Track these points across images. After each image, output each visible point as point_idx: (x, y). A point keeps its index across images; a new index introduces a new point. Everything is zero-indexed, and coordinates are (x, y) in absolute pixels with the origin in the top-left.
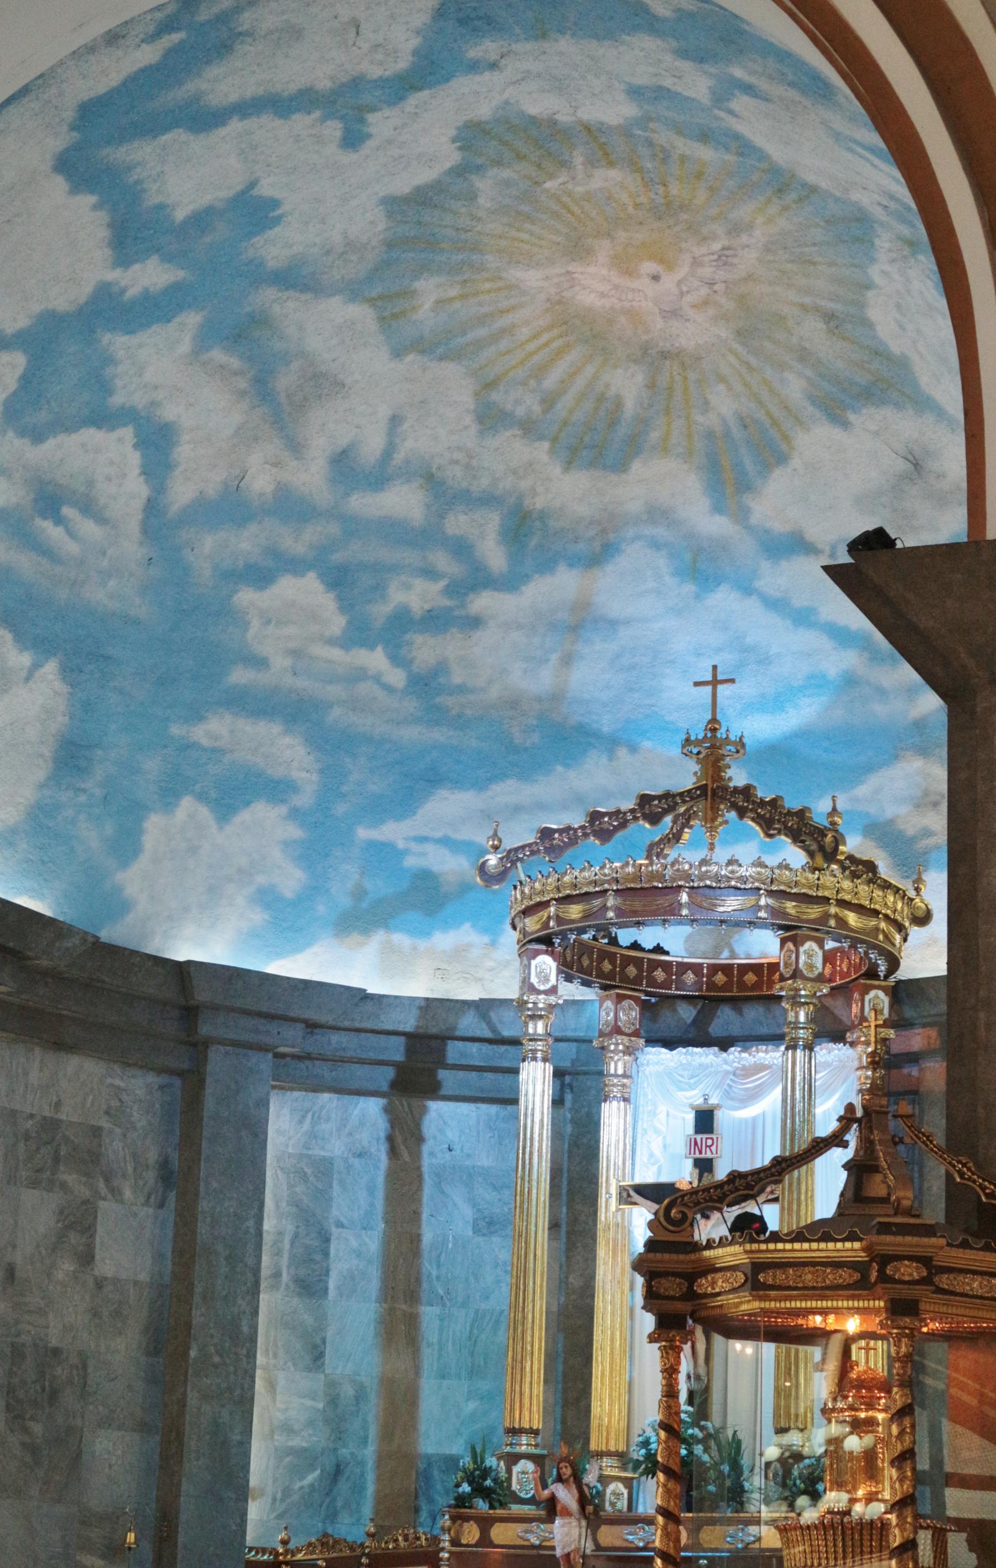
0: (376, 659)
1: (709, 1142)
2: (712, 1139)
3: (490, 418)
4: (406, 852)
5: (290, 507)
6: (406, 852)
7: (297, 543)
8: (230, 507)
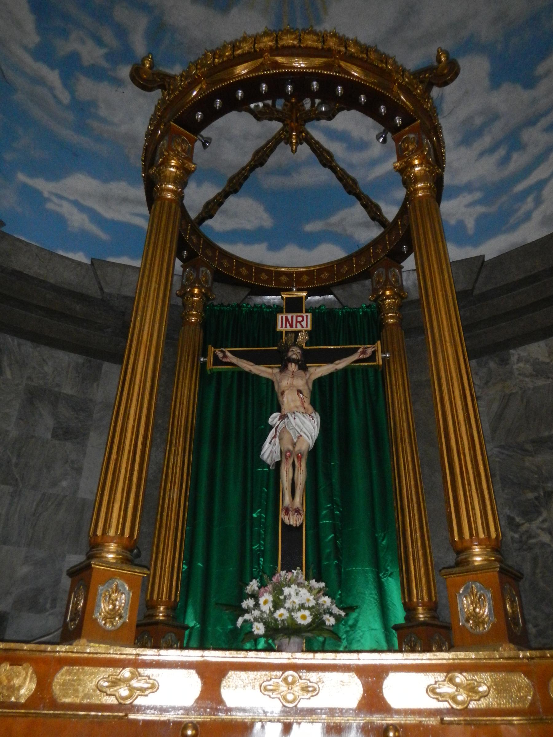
0: (54, 77)
1: (300, 319)
2: (303, 317)
4: (48, 200)
6: (48, 200)
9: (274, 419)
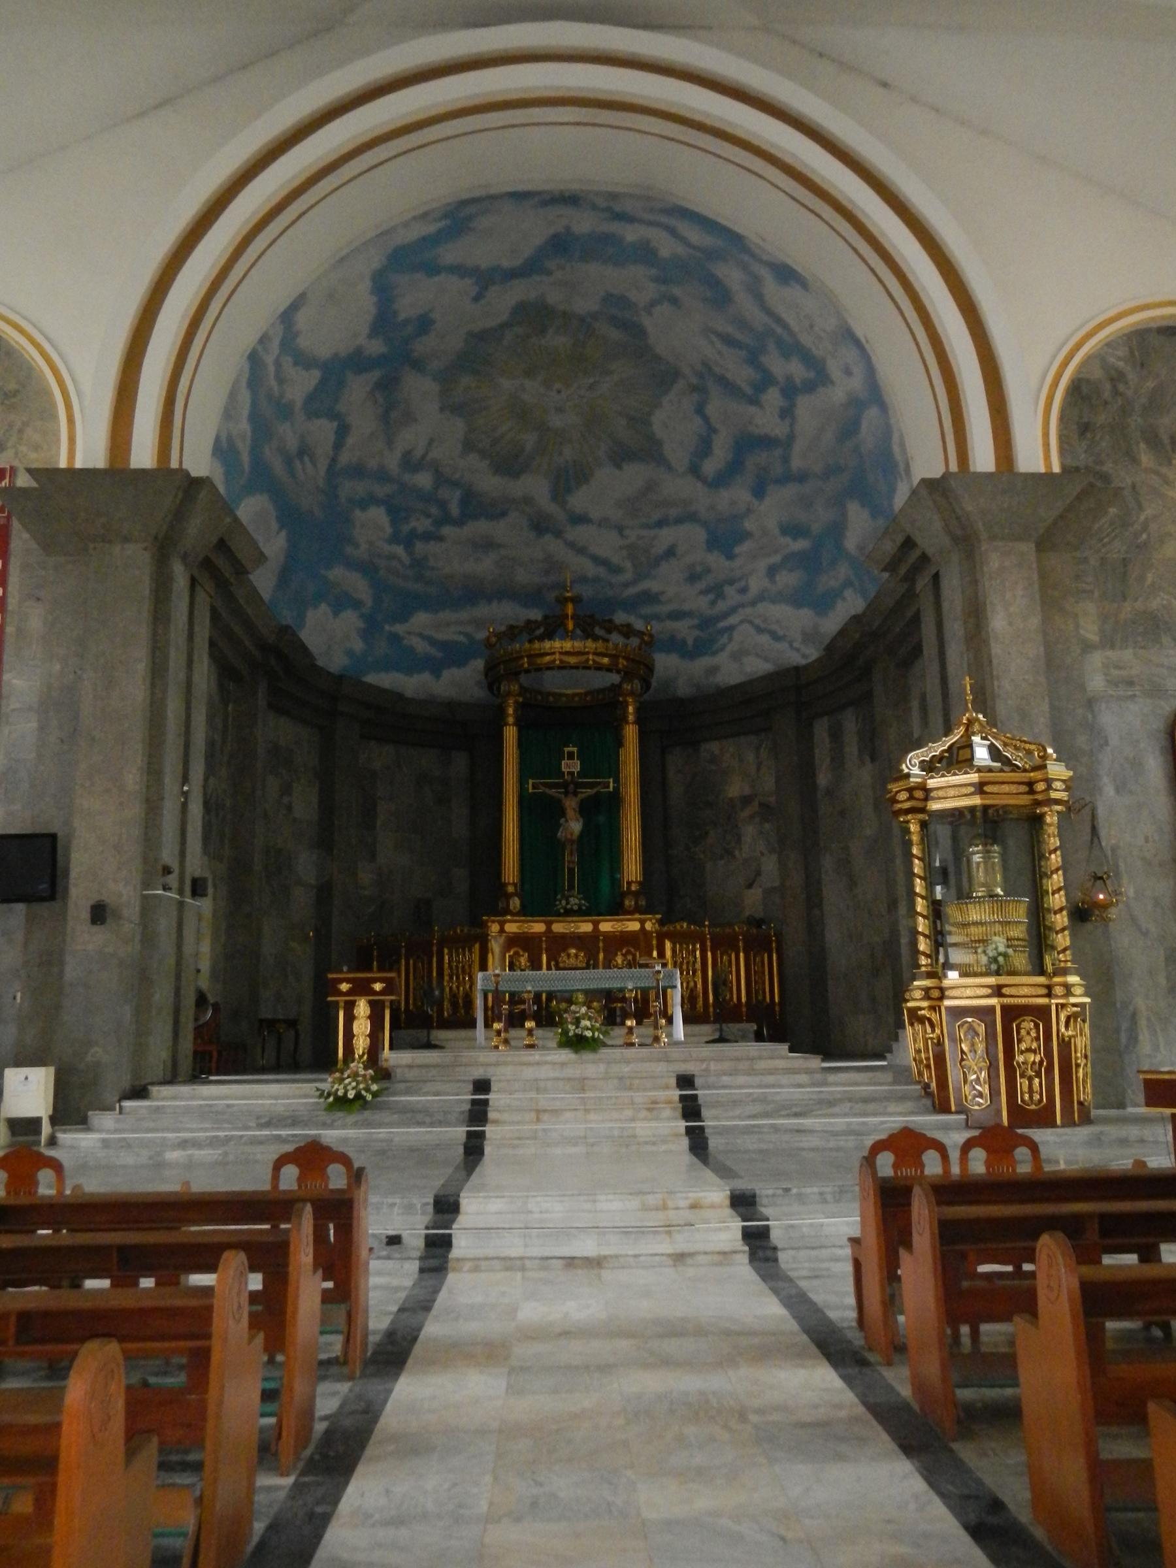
0: (400, 550)
3: (469, 446)
5: (382, 476)
7: (381, 491)
8: (358, 471)
9: (562, 821)
